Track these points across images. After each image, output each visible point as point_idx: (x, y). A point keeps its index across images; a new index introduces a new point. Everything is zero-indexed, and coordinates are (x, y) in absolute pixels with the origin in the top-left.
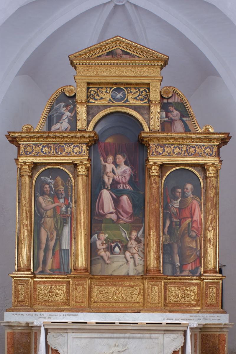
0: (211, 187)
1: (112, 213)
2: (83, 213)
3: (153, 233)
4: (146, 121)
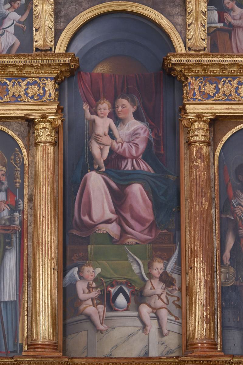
1: (109, 221)
2: (48, 224)
3: (199, 265)
4: (177, 30)
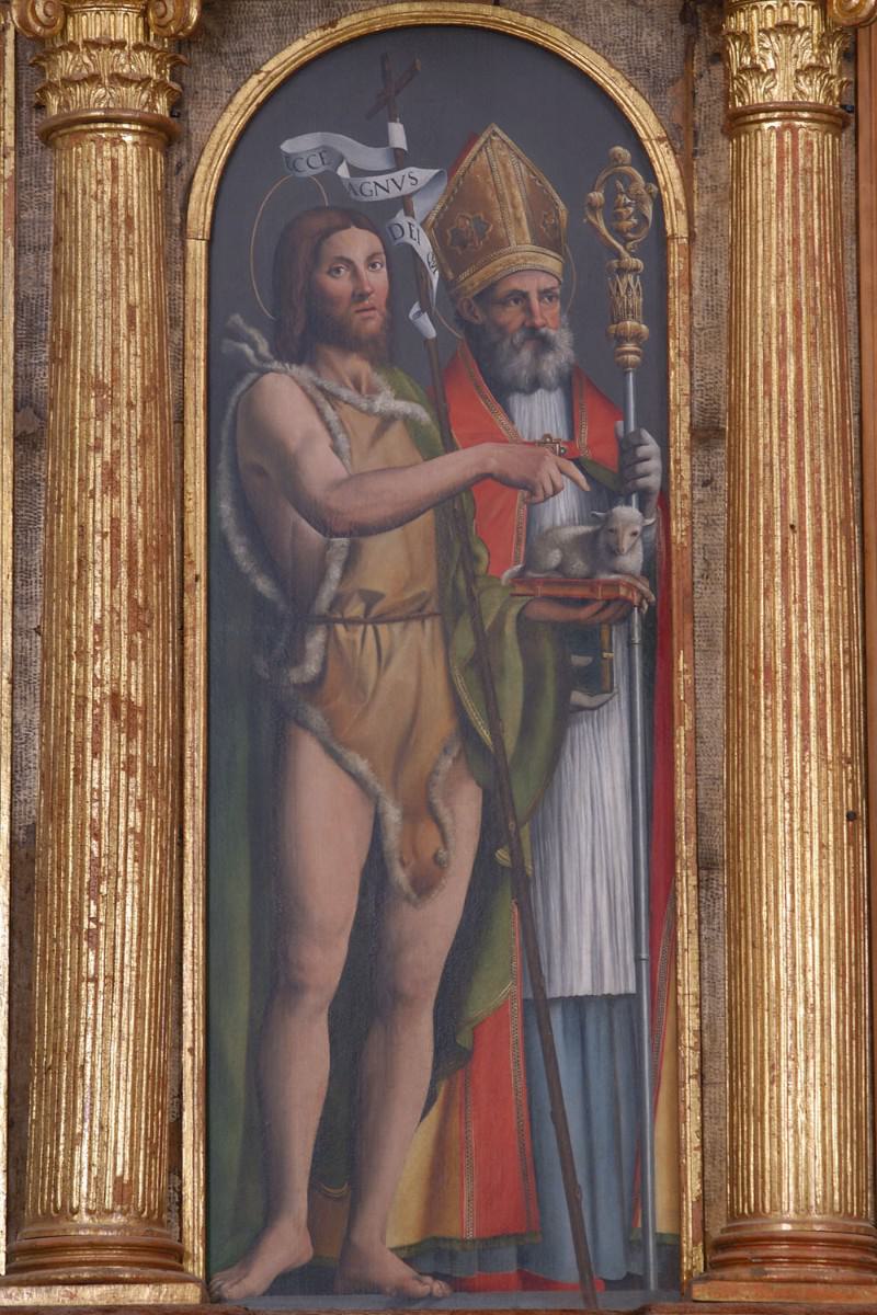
2: (818, 566)
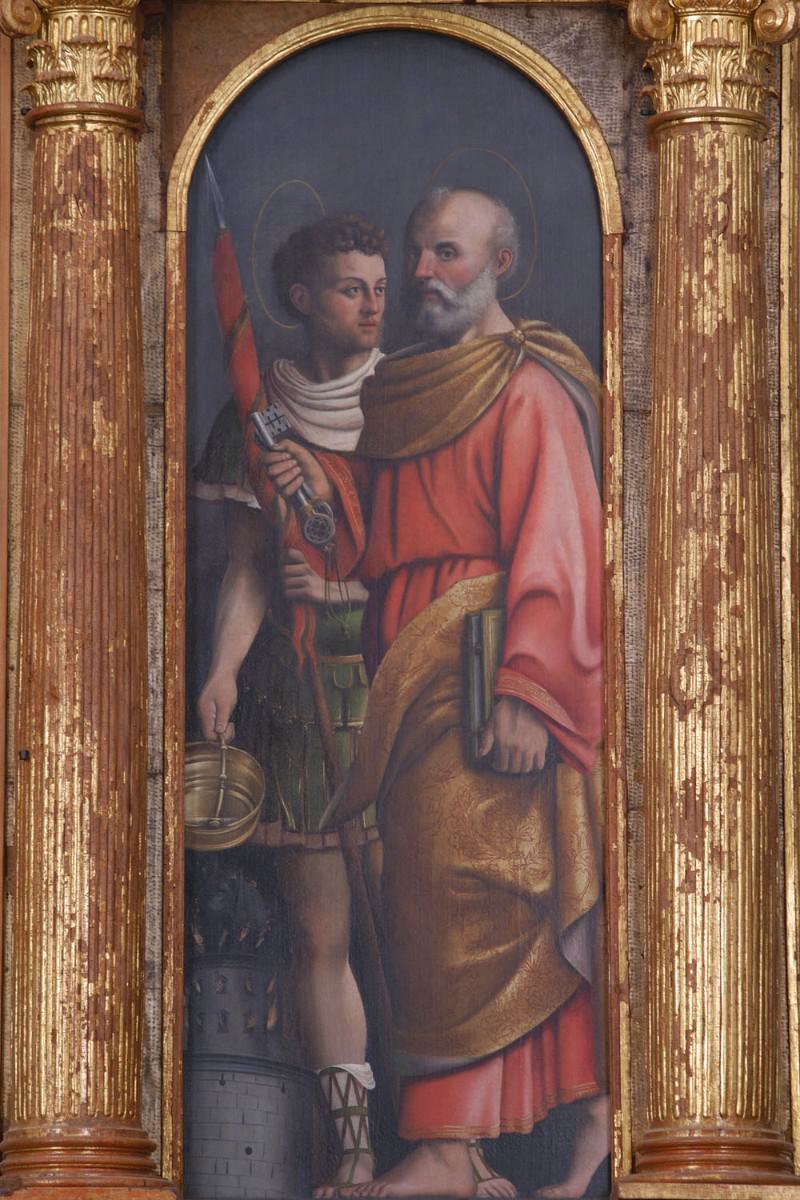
0: (702, 228)
